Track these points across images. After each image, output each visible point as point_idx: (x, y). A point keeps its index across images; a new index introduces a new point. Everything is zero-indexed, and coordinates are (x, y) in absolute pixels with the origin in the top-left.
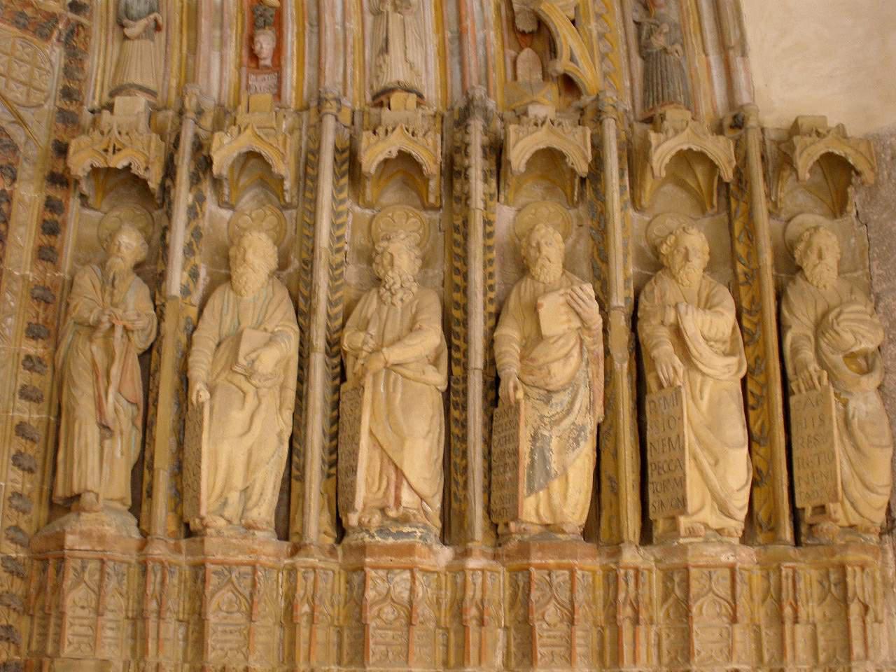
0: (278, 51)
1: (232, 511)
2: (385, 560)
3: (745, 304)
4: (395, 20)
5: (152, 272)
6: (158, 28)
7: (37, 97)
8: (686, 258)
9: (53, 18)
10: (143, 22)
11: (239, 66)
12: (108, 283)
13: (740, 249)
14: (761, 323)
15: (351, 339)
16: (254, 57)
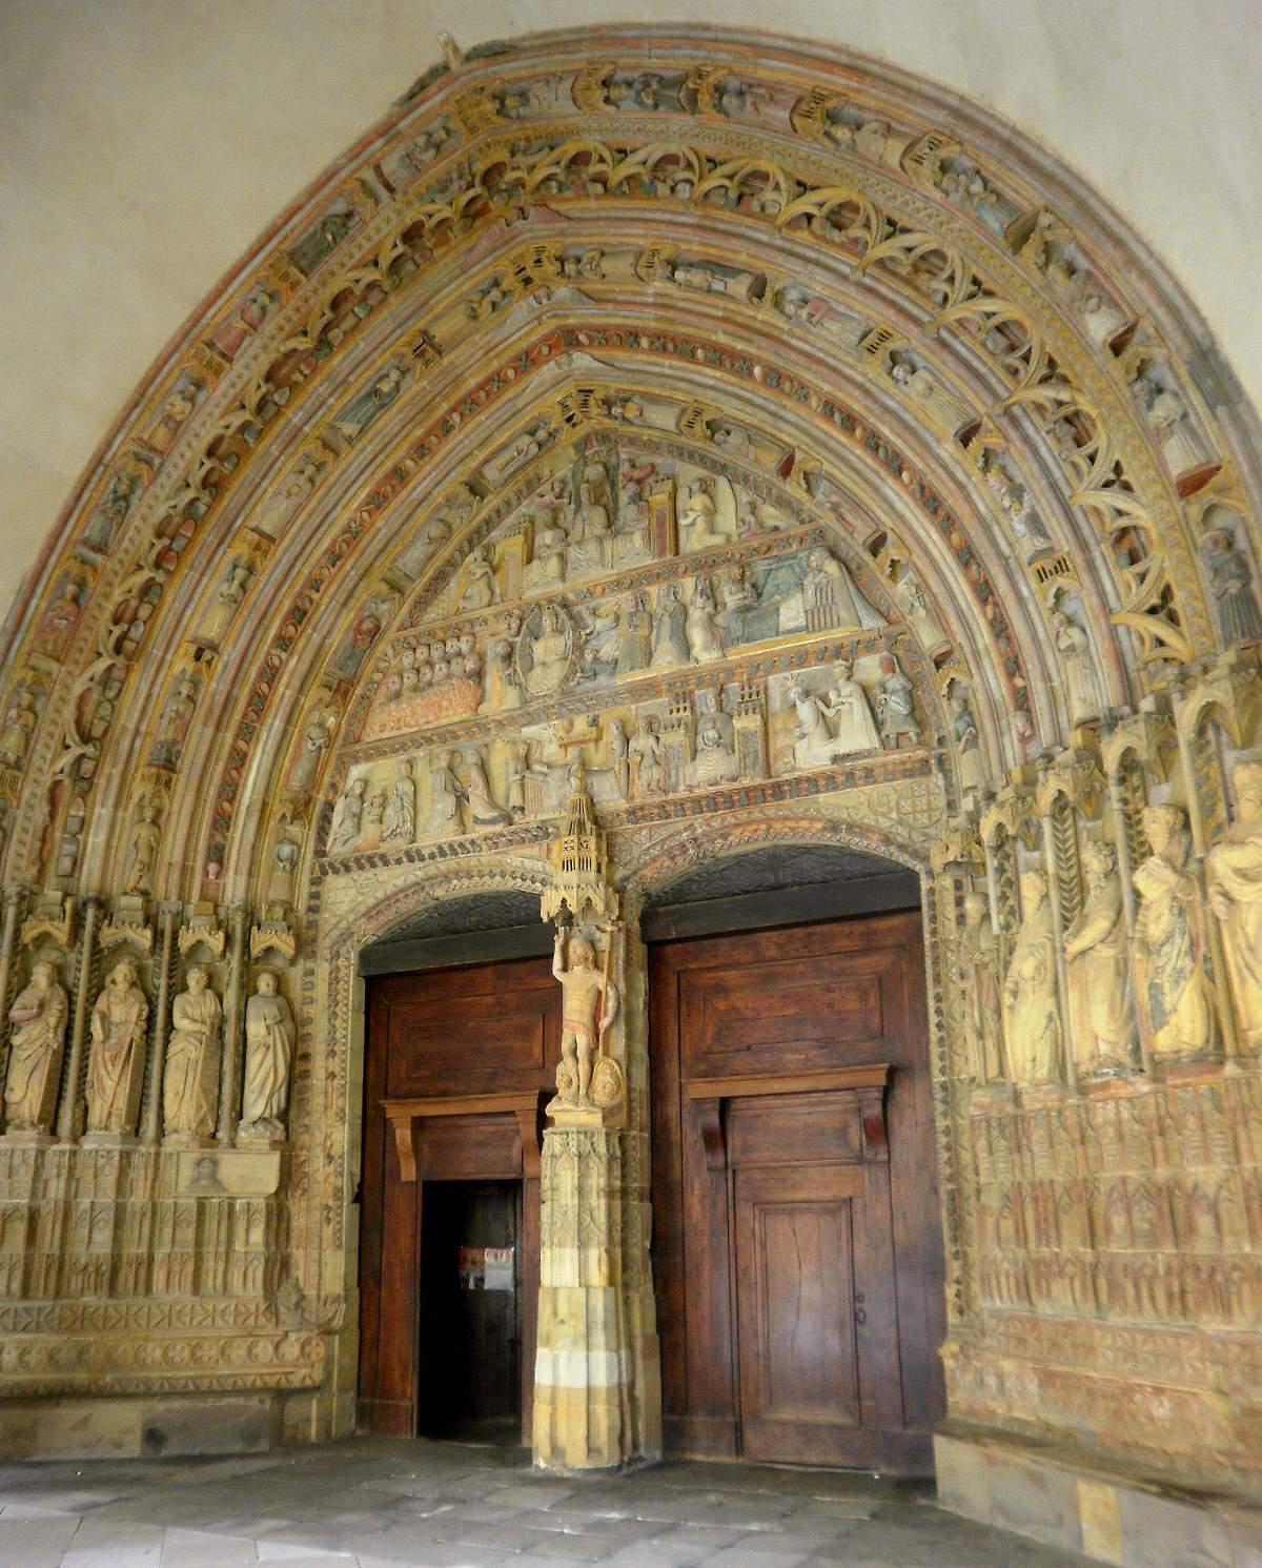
1: (1028, 1076)
2: (1100, 1094)
7: (936, 816)
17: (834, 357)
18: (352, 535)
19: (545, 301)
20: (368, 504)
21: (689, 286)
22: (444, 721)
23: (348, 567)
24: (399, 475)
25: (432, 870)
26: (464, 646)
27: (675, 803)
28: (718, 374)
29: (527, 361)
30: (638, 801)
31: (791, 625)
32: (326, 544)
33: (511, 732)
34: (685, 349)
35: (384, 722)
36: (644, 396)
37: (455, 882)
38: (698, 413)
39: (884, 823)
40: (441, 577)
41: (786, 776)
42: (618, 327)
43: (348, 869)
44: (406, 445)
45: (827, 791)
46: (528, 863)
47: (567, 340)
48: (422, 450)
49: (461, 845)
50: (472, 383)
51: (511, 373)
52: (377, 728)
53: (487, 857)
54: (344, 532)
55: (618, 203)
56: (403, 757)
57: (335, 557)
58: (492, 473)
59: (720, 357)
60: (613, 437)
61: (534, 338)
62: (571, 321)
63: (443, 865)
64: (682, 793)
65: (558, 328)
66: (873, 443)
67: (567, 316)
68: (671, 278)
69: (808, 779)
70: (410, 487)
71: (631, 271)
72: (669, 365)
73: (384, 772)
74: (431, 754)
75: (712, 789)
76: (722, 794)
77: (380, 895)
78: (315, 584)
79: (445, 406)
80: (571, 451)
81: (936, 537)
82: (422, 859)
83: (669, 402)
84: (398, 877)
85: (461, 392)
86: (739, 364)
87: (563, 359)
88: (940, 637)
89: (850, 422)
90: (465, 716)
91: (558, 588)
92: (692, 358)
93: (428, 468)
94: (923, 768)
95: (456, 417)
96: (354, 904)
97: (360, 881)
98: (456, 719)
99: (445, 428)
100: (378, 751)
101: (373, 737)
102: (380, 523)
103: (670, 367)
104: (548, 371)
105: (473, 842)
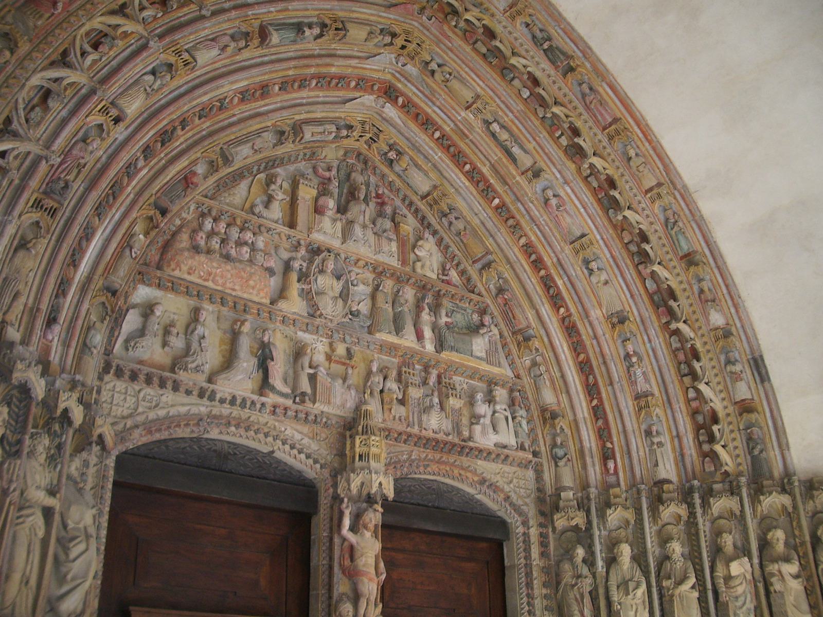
0: (616, 467)
3: (801, 554)
4: (658, 451)
5: (590, 562)
6: (569, 460)
8: (778, 540)
9: (531, 461)
10: (565, 460)
11: (602, 474)
12: (574, 567)
13: (797, 533)
14: (808, 562)
15: (665, 583)
16: (607, 470)
17: (550, 229)
18: (222, 105)
19: (400, 65)
20: (241, 93)
21: (494, 135)
22: (245, 296)
23: (204, 126)
24: (264, 90)
25: (215, 411)
26: (260, 244)
27: (410, 435)
28: (467, 183)
29: (364, 84)
30: (389, 425)
31: (479, 354)
32: (205, 99)
33: (290, 331)
34: (458, 158)
35: (190, 268)
36: (412, 159)
37: (233, 429)
38: (444, 195)
39: (507, 489)
40: (238, 176)
41: (471, 444)
42: (427, 114)
43: (134, 377)
44: (281, 74)
45: (485, 459)
46: (298, 436)
47: (389, 93)
48: (285, 86)
49: (253, 403)
50: (333, 70)
51: (353, 84)
52: (185, 268)
53: (265, 418)
54: (219, 101)
55: (481, 62)
56: (193, 302)
57: (204, 113)
58: (308, 133)
59: (474, 176)
60: (370, 164)
61: (375, 75)
62: (399, 85)
63: (226, 410)
64: (415, 430)
65: (390, 82)
66: (547, 283)
67: (399, 81)
68: (487, 123)
69: (480, 451)
70: (262, 103)
71: (471, 100)
72: (438, 155)
73: (173, 306)
74: (219, 312)
75: (431, 435)
76: (437, 441)
77: (162, 413)
78: (184, 123)
79: (312, 70)
80: (341, 152)
81: (566, 348)
82: (212, 398)
83: (426, 174)
84: (183, 405)
85: (324, 70)
86: (487, 192)
87: (382, 100)
88: (555, 401)
89: (538, 264)
90: (264, 301)
91: (336, 243)
92: (460, 165)
93: (279, 99)
94: (525, 465)
95: (314, 82)
96: (131, 411)
97: (142, 395)
98: (256, 299)
99: (303, 83)
100: (173, 286)
101: (177, 273)
102: (236, 111)
103: (440, 158)
104: (368, 99)
105: (263, 405)
